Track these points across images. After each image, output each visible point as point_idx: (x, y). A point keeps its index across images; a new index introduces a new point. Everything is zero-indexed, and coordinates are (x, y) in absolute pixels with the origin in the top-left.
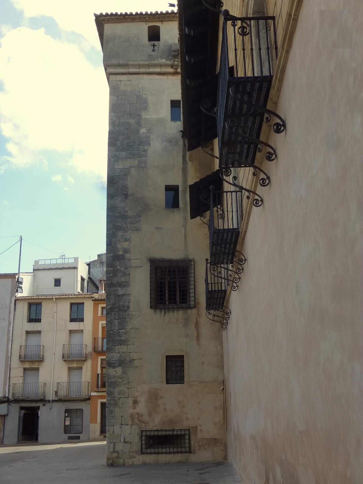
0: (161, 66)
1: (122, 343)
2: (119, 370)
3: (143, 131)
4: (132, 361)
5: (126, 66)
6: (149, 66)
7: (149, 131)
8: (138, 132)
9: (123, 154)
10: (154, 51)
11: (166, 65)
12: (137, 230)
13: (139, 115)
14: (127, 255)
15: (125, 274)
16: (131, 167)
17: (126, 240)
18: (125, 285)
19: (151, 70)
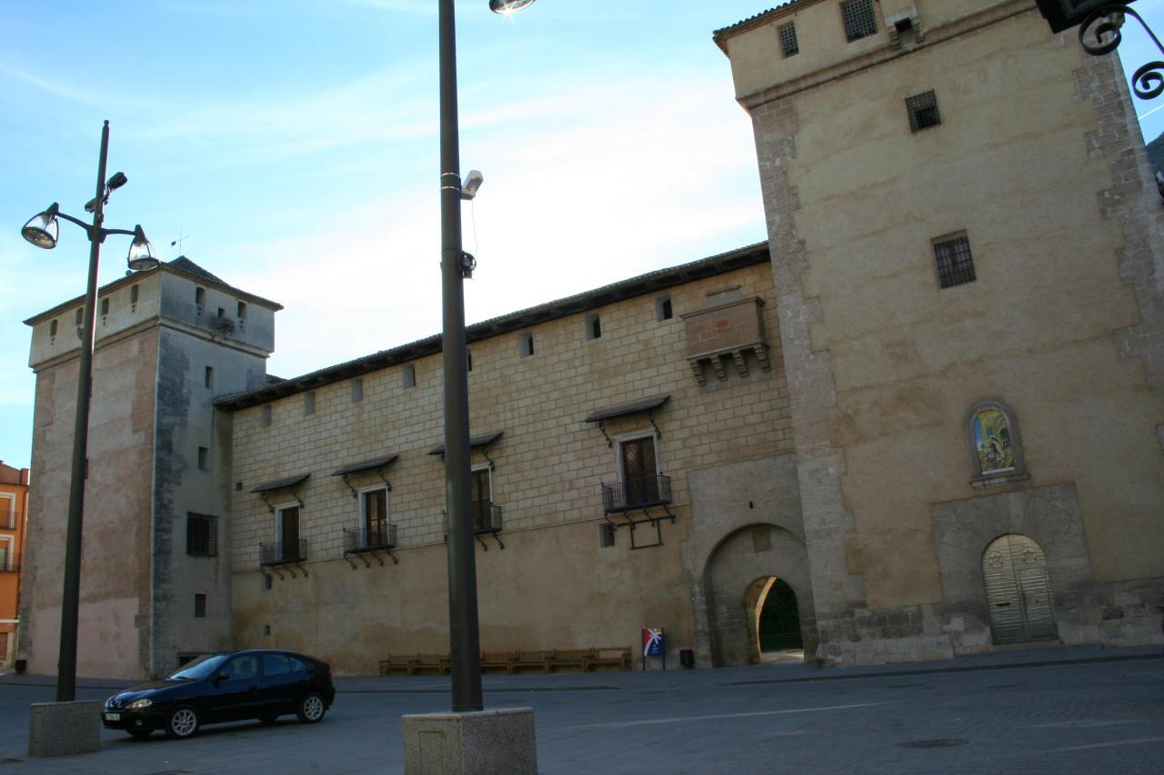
0: (203, 331)
1: (165, 581)
2: (163, 603)
3: (185, 391)
4: (172, 596)
5: (177, 322)
6: (194, 328)
7: (190, 392)
8: (180, 390)
9: (169, 409)
10: (199, 314)
11: (206, 332)
12: (179, 484)
13: (183, 374)
14: (171, 506)
15: (169, 522)
16: (174, 424)
17: (170, 492)
18: (168, 531)
19: (195, 332)
